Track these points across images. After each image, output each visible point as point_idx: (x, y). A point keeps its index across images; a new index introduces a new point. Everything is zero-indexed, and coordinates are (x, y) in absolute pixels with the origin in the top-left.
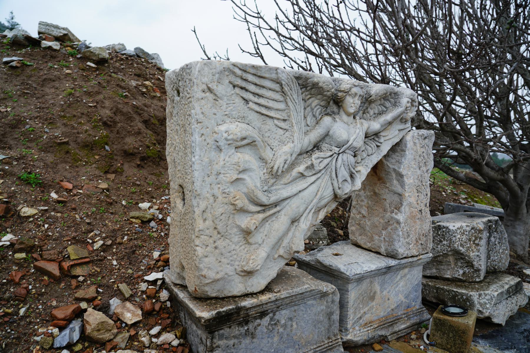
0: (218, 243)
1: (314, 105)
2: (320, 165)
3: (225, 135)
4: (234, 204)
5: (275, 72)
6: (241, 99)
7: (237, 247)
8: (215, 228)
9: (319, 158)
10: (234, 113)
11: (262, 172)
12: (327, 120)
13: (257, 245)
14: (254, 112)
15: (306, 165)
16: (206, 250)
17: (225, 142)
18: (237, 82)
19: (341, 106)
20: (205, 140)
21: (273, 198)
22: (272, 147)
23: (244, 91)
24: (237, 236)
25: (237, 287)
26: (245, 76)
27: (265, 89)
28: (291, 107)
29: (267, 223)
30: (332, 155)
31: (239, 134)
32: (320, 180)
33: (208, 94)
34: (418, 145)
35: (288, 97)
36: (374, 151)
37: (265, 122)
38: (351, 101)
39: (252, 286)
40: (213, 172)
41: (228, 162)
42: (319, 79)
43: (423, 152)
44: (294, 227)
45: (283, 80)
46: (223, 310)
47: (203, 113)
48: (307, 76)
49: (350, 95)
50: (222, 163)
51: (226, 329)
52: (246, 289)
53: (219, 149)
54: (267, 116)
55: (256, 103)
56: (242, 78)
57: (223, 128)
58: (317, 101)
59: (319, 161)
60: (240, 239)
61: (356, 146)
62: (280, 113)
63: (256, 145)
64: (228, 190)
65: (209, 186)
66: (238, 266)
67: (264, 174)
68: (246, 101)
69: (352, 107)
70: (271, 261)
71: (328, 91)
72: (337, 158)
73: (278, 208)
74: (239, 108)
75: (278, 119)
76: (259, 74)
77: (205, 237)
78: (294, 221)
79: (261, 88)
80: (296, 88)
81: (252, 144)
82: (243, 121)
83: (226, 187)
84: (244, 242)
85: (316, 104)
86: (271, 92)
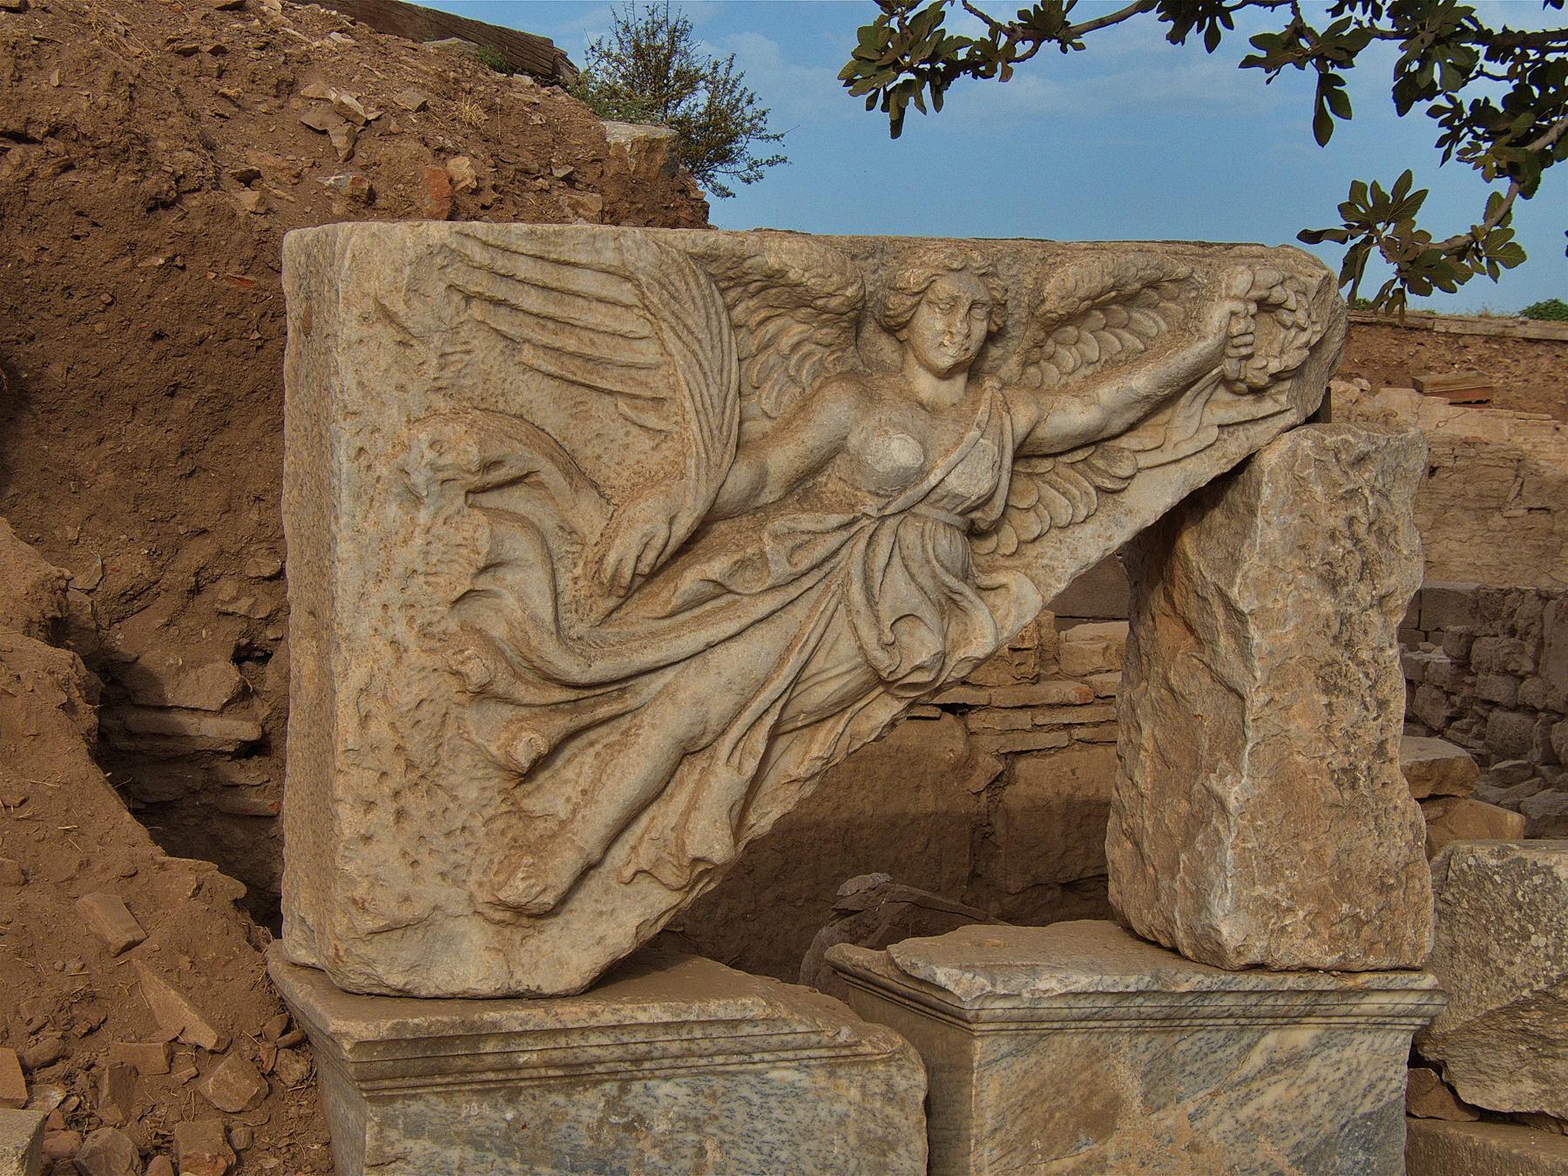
1: (785, 343)
4: (456, 673)
5: (612, 245)
9: (792, 532)
10: (468, 382)
14: (539, 377)
15: (737, 557)
17: (430, 474)
23: (503, 310)
24: (476, 783)
26: (502, 263)
28: (677, 357)
29: (592, 751)
32: (799, 611)
33: (379, 327)
35: (664, 325)
49: (930, 302)
51: (433, 1099)
52: (511, 974)
55: (545, 347)
56: (492, 272)
58: (798, 328)
61: (960, 490)
63: (540, 485)
67: (575, 580)
69: (942, 344)
71: (830, 295)
76: (553, 256)
77: (367, 773)
80: (695, 292)
83: (435, 619)
84: (504, 808)
85: (796, 339)
86: (602, 308)
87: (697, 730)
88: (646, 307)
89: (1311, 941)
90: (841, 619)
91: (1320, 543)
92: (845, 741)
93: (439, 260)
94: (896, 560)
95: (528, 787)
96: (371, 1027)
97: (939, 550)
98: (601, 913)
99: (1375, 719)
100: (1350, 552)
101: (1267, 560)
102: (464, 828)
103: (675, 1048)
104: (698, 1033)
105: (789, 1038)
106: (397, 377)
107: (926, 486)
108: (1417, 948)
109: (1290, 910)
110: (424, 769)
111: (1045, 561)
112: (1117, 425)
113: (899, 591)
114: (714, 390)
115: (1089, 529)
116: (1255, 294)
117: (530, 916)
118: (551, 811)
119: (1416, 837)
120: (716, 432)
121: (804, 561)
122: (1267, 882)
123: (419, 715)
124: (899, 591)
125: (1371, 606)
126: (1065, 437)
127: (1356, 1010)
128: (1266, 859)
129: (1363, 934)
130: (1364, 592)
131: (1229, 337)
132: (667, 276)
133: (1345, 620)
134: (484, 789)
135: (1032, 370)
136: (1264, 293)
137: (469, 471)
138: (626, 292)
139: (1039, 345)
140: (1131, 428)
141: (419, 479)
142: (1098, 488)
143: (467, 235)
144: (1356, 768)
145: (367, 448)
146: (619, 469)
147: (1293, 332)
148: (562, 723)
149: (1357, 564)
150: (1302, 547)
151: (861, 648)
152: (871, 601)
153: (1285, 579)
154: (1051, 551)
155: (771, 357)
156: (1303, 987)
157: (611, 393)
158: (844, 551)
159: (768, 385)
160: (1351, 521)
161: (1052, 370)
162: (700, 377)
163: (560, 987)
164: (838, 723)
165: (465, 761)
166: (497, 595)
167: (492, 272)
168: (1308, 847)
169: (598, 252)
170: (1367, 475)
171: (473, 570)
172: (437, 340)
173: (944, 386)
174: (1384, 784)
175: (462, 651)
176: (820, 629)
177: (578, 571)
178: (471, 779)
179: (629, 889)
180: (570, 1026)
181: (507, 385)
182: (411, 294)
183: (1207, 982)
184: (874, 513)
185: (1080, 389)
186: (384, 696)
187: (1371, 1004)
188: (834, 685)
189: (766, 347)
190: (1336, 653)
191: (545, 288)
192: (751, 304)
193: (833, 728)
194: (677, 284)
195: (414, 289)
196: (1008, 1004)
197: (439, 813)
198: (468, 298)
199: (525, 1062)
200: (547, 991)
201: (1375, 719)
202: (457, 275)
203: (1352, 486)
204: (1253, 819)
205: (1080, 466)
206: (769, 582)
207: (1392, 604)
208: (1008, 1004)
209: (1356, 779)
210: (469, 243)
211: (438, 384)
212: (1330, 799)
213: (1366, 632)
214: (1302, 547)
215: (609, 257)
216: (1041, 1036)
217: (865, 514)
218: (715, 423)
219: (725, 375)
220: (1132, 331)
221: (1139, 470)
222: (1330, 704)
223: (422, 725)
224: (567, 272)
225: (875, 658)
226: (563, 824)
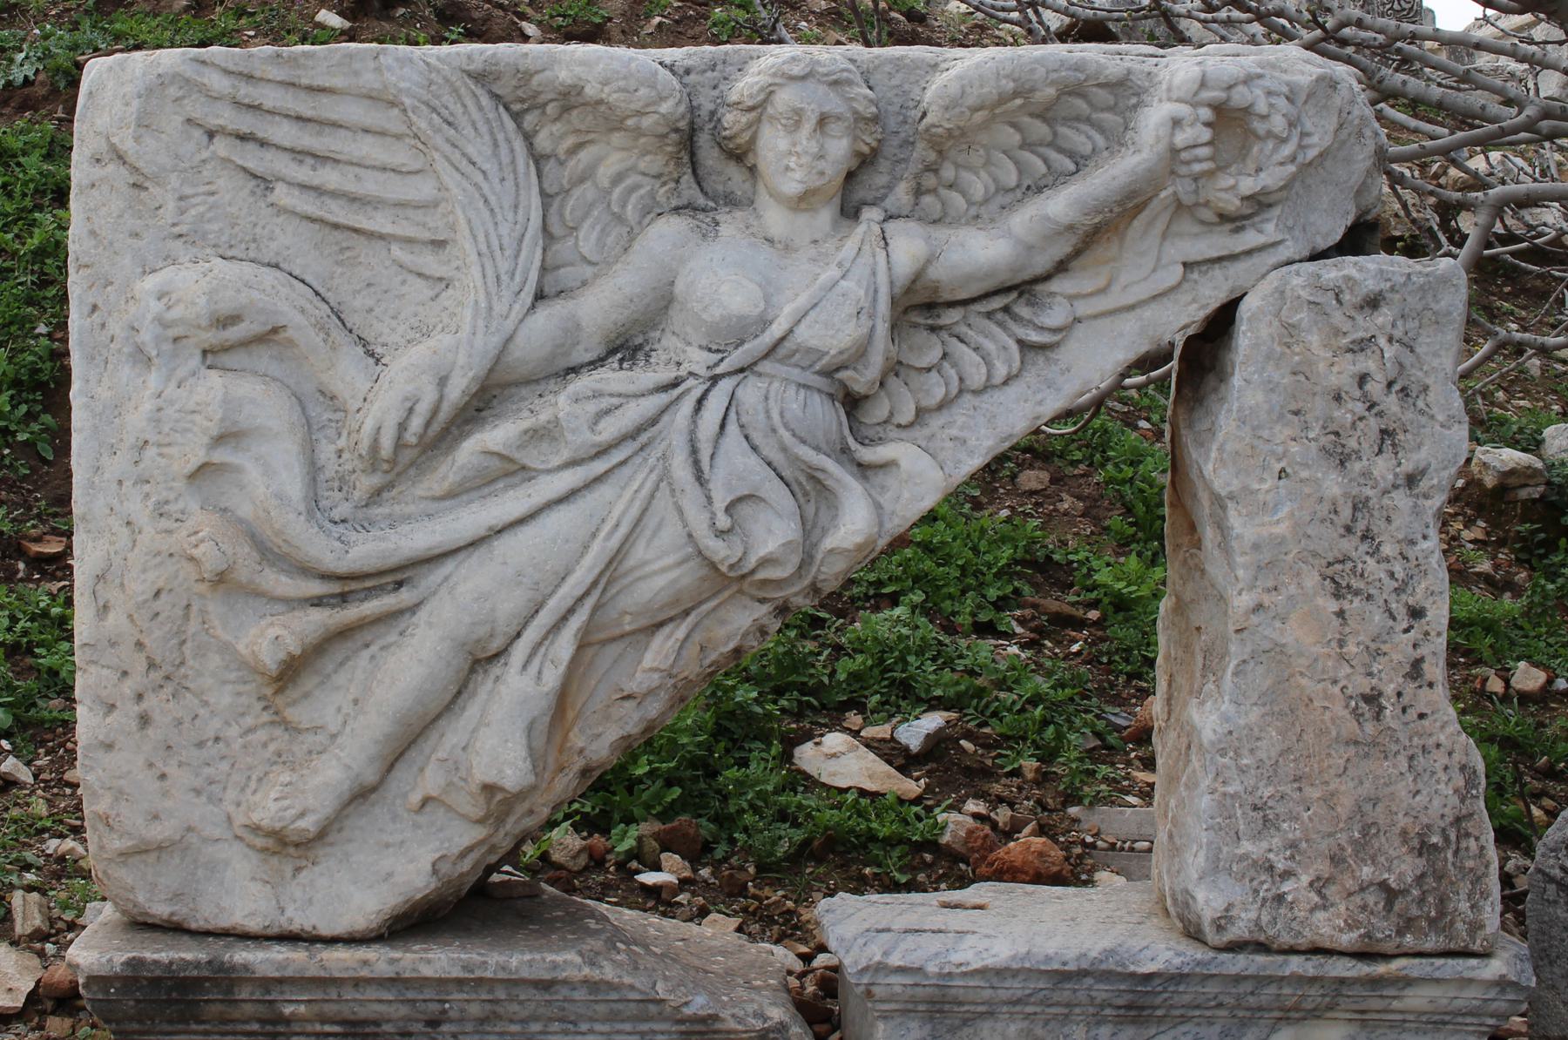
0: (152, 702)
1: (605, 173)
2: (602, 425)
3: (156, 307)
4: (192, 559)
5: (372, 65)
6: (242, 174)
7: (233, 731)
8: (140, 645)
10: (215, 227)
11: (332, 448)
12: (668, 231)
13: (321, 738)
16: (108, 720)
18: (218, 116)
19: (755, 166)
20: (103, 325)
21: (365, 551)
22: (379, 350)
23: (250, 146)
24: (230, 687)
25: (241, 895)
26: (246, 92)
27: (342, 132)
28: (455, 191)
29: (366, 654)
30: (675, 384)
31: (202, 301)
32: (605, 491)
34: (1314, 339)
35: (436, 156)
36: (1001, 371)
37: (348, 254)
38: (783, 144)
39: (310, 901)
40: (125, 437)
41: (172, 403)
42: (578, 70)
43: (1363, 379)
44: (489, 684)
45: (408, 92)
46: (156, 956)
47: (93, 233)
48: (528, 64)
49: (772, 117)
50: (148, 406)
52: (283, 911)
53: (141, 358)
54: (356, 230)
55: (304, 187)
56: (237, 104)
57: (151, 283)
59: (592, 407)
60: (244, 700)
61: (813, 343)
62: (418, 216)
63: (291, 343)
64: (180, 505)
65: (114, 486)
66: (238, 805)
68: (264, 182)
69: (787, 168)
70: (395, 818)
71: (640, 113)
72: (700, 402)
73: (405, 596)
74: (234, 210)
75: (409, 241)
76: (305, 81)
77: (105, 672)
78: (481, 660)
79: (327, 130)
80: (476, 115)
81: (270, 336)
82: (252, 255)
83: (172, 496)
86: (369, 139)
87: (482, 631)
88: (416, 136)
89: (1320, 915)
90: (663, 502)
91: (1319, 407)
92: (692, 650)
93: (173, 91)
94: (732, 427)
95: (292, 693)
96: (104, 960)
97: (788, 416)
98: (387, 846)
99: (1406, 631)
100: (1361, 419)
101: (1247, 428)
102: (217, 739)
103: (475, 1010)
104: (501, 994)
105: (620, 1006)
106: (131, 223)
107: (768, 338)
108: (1475, 927)
109: (1287, 875)
110: (167, 669)
111: (954, 432)
112: (1042, 263)
113: (736, 466)
114: (504, 229)
115: (1013, 390)
116: (1206, 95)
117: (297, 845)
118: (319, 723)
119: (1470, 783)
120: (504, 278)
121: (610, 429)
122: (1257, 836)
123: (158, 605)
124: (736, 466)
125: (1395, 487)
126: (970, 278)
127: (1396, 1004)
128: (1255, 808)
129: (1396, 908)
130: (1383, 468)
131: (1174, 152)
132: (438, 97)
133: (1359, 505)
134: (239, 694)
135: (927, 200)
136: (1221, 95)
137: (199, 327)
138: (390, 120)
139: (932, 169)
140: (1061, 267)
141: (146, 337)
142: (1020, 342)
143: (204, 62)
144: (1380, 694)
145: (100, 304)
146: (394, 323)
147: (1270, 145)
148: (318, 620)
149: (1374, 434)
150: (1296, 413)
151: (690, 536)
152: (700, 478)
153: (1273, 453)
155: (587, 191)
156: (1311, 972)
157: (382, 237)
158: (666, 418)
159: (586, 225)
160: (1363, 379)
161: (956, 199)
162: (486, 214)
163: (340, 927)
164: (678, 627)
165: (215, 661)
166: (237, 469)
167: (237, 104)
168: (1314, 793)
169: (356, 73)
170: (1380, 320)
171: (206, 440)
172: (174, 180)
173: (802, 219)
174: (1422, 716)
175: (196, 533)
176: (635, 511)
177: (342, 443)
178: (225, 682)
179: (421, 819)
180: (337, 975)
181: (258, 230)
182: (143, 130)
183: (1177, 961)
184: (703, 372)
185: (992, 220)
186: (122, 585)
187: (1416, 999)
188: (660, 582)
189: (582, 180)
190: (1348, 545)
191: (299, 118)
192: (554, 129)
193: (672, 633)
194: (451, 106)
195: (144, 124)
196: (908, 980)
197: (187, 719)
198: (211, 135)
199: (292, 1013)
200: (325, 931)
201: (1406, 631)
202: (196, 108)
203: (1361, 334)
205: (1000, 316)
206: (566, 454)
207: (1424, 485)
208: (908, 980)
209: (1382, 708)
210: (206, 70)
211: (176, 230)
212: (1344, 733)
213: (1388, 520)
214: (1296, 413)
215: (369, 80)
216: (965, 1022)
217: (691, 373)
218: (504, 266)
219: (521, 212)
220: (1060, 150)
221: (1078, 320)
222: (1341, 614)
223: (160, 618)
224: (325, 99)
225: (707, 548)
226: (334, 737)
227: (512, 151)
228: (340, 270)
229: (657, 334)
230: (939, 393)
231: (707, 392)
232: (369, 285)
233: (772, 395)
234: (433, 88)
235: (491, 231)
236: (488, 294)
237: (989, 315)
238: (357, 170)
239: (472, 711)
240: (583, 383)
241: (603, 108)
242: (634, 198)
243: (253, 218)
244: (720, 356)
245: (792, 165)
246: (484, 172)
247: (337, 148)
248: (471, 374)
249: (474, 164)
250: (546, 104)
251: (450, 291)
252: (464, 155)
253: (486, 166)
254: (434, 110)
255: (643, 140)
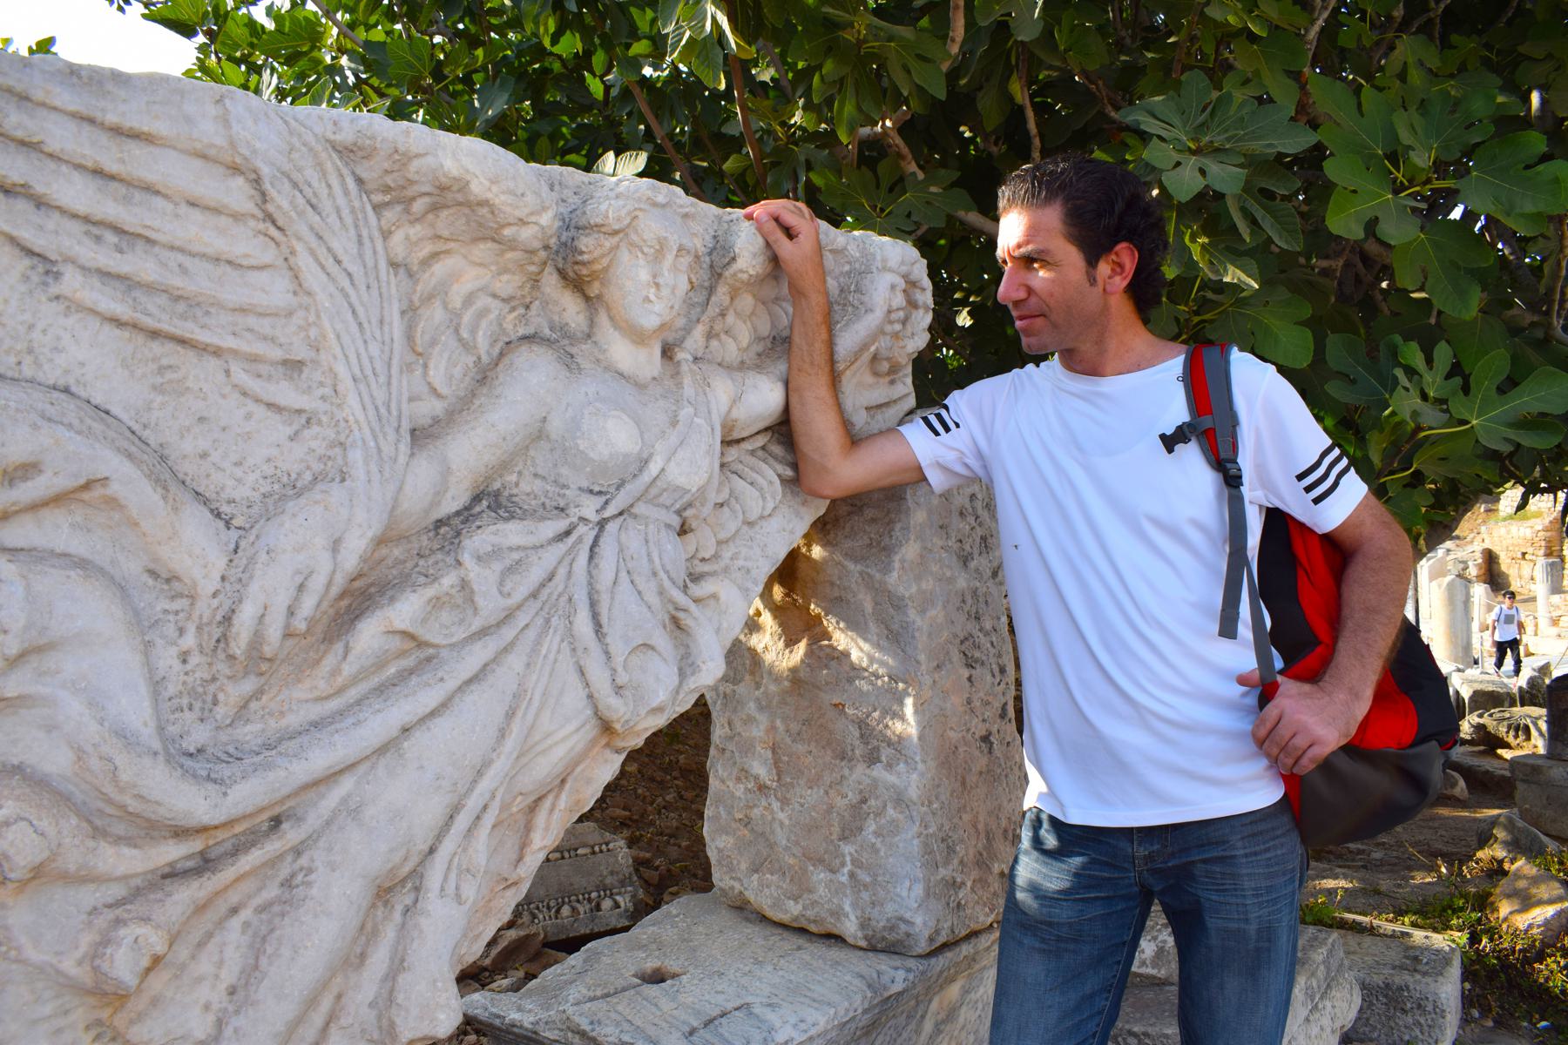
9: (496, 553)
11: (174, 651)
14: (95, 323)
19: (599, 297)
22: (225, 508)
30: (568, 533)
32: (515, 662)
37: (169, 375)
54: (182, 341)
55: (105, 275)
61: (681, 481)
68: (46, 265)
71: (522, 222)
79: (138, 196)
80: (341, 201)
111: (741, 563)
114: (374, 349)
120: (383, 411)
135: (714, 343)
146: (238, 472)
151: (590, 696)
154: (744, 551)
157: (217, 352)
162: (354, 328)
181: (36, 335)
191: (98, 173)
194: (315, 184)
204: (930, 803)
205: (760, 453)
206: (477, 624)
222: (970, 679)
227: (375, 252)
228: (159, 399)
229: (514, 478)
230: (732, 526)
231: (597, 538)
232: (201, 420)
233: (650, 537)
234: (295, 155)
235: (362, 350)
236: (372, 430)
237: (753, 453)
238: (181, 258)
239: (379, 959)
240: (480, 540)
241: (484, 211)
242: (484, 324)
243: (27, 317)
244: (603, 499)
245: (652, 297)
246: (349, 275)
247: (156, 224)
248: (370, 534)
249: (339, 263)
250: (413, 199)
251: (315, 429)
252: (329, 249)
253: (352, 268)
254: (295, 185)
255: (509, 255)
